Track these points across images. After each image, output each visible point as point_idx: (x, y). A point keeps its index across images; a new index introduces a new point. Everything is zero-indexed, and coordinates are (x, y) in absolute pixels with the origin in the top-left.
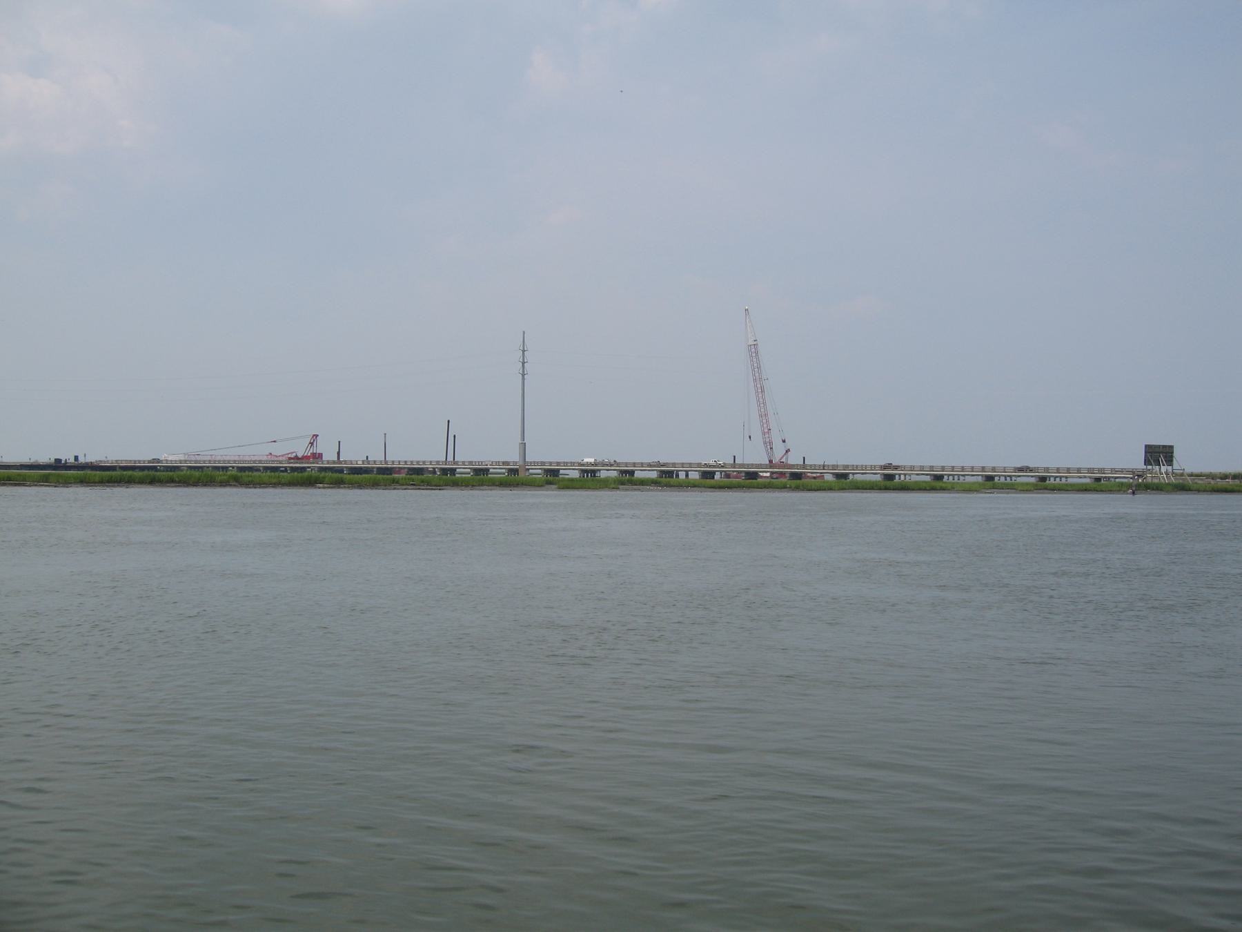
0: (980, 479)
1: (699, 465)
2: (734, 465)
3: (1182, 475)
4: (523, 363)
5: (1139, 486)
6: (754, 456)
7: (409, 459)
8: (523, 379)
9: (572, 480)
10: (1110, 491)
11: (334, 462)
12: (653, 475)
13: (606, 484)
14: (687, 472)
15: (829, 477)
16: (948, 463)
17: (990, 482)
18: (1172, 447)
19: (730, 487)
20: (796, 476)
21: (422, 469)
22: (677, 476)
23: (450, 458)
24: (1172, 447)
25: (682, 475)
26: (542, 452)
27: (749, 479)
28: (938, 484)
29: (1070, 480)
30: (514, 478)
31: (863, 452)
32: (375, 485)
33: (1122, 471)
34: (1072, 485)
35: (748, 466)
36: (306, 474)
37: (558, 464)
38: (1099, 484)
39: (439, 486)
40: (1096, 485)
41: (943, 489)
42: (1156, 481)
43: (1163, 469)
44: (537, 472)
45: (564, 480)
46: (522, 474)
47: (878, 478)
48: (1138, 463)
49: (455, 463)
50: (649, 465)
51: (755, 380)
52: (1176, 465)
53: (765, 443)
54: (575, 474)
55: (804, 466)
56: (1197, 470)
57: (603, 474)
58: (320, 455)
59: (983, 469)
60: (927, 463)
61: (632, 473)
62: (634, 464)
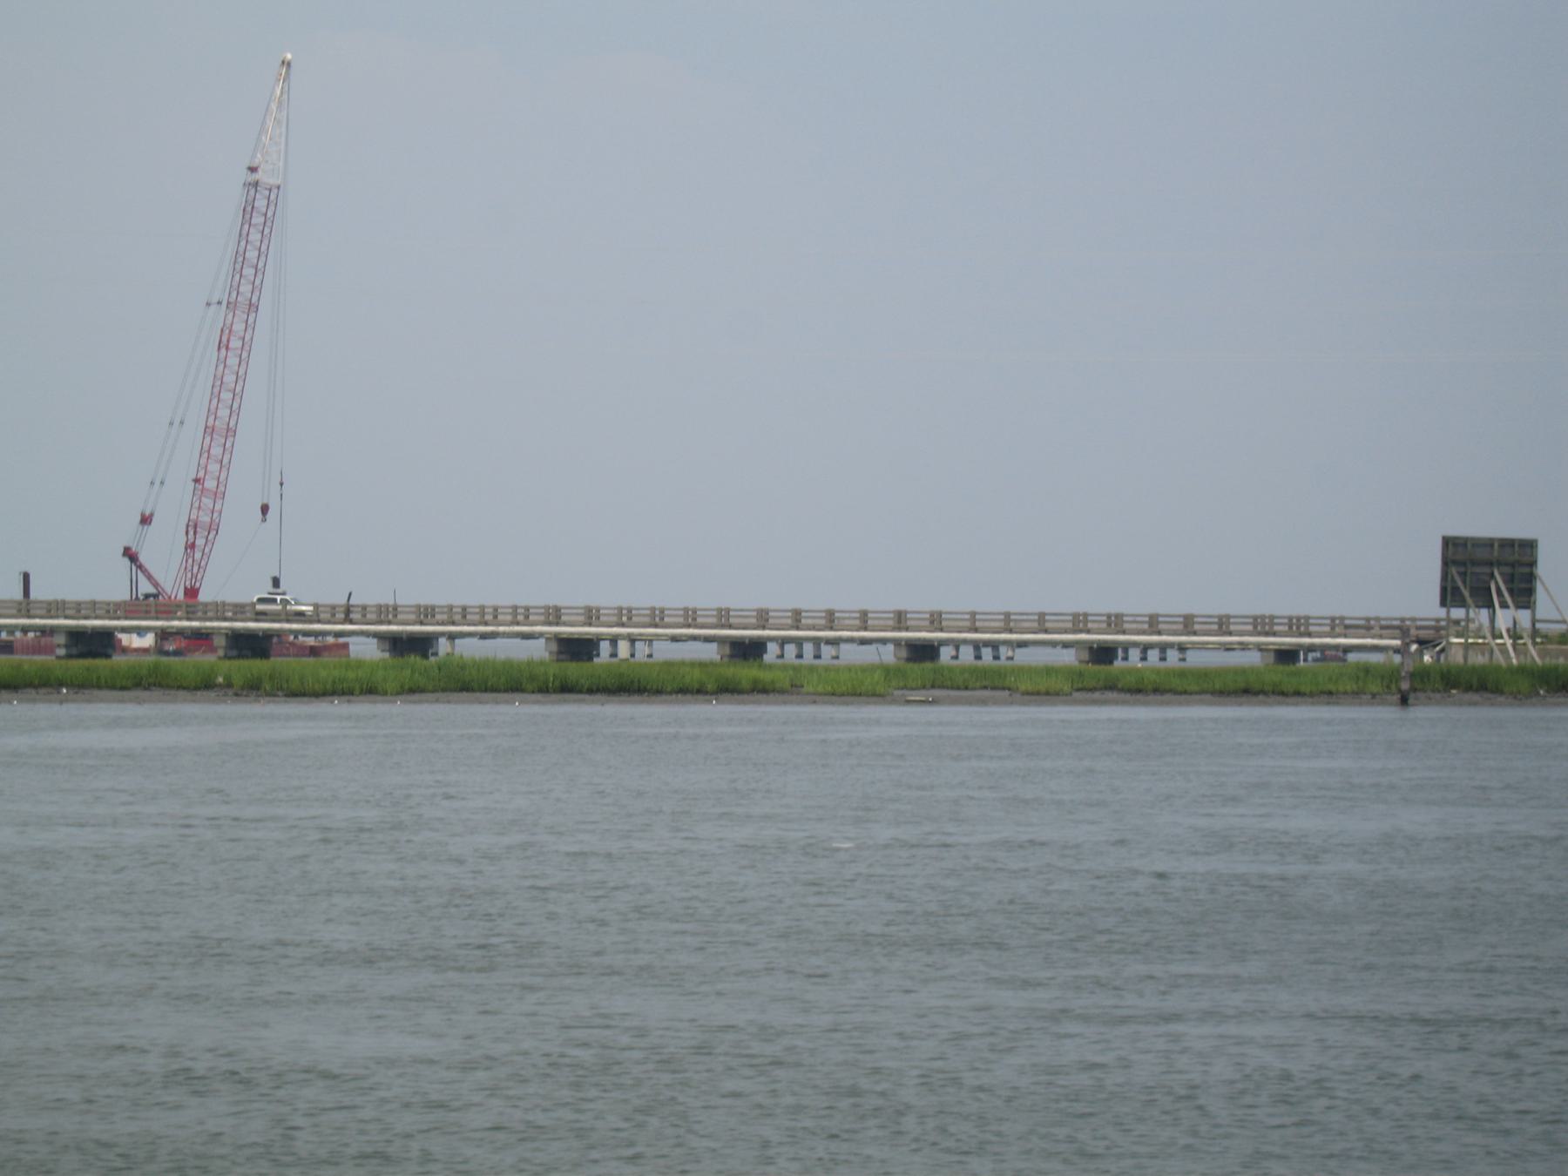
0: (888, 655)
5: (1422, 677)
10: (1327, 695)
16: (780, 600)
18: (1529, 546)
24: (1529, 546)
29: (1195, 659)
33: (1366, 627)
34: (1203, 675)
38: (1292, 671)
40: (1279, 674)
41: (761, 690)
42: (1478, 659)
43: (1504, 619)
48: (1420, 597)
52: (1544, 605)
59: (900, 620)
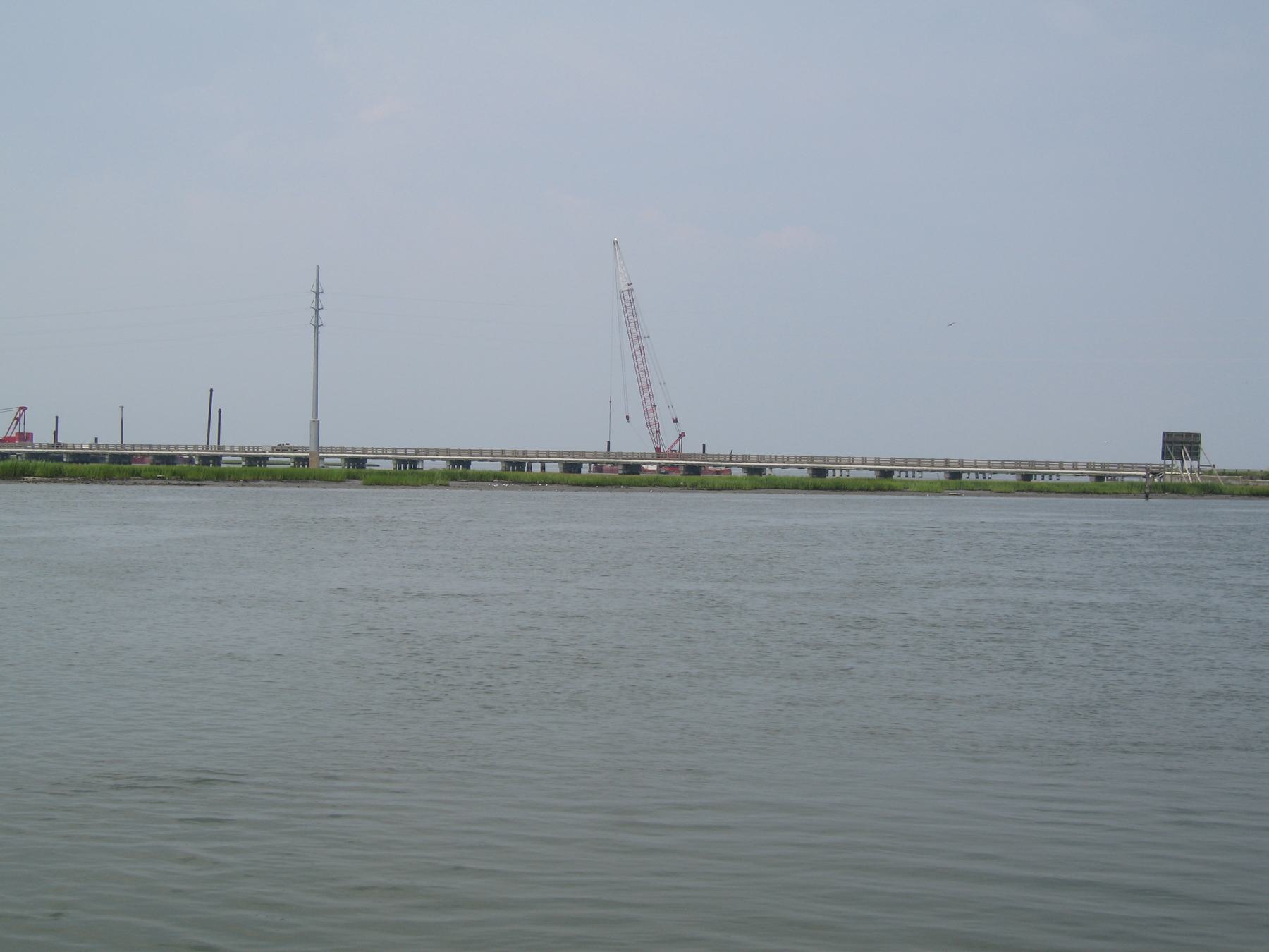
0: (942, 476)
1: (560, 454)
2: (608, 454)
3: (1211, 473)
4: (317, 310)
5: (1153, 487)
6: (633, 441)
7: (155, 442)
8: (317, 333)
9: (384, 473)
10: (1116, 494)
11: (50, 446)
12: (497, 467)
13: (430, 479)
14: (543, 463)
15: (738, 472)
16: (900, 454)
17: (956, 480)
18: (1198, 435)
19: (602, 484)
20: (694, 470)
21: (173, 457)
22: (530, 468)
23: (213, 442)
24: (1198, 435)
25: (536, 468)
26: (344, 434)
27: (629, 474)
28: (886, 482)
29: (1063, 479)
30: (302, 470)
31: (789, 439)
32: (106, 478)
33: (1132, 467)
34: (1067, 485)
35: (627, 455)
36: (9, 463)
37: (365, 450)
38: (1102, 484)
39: (198, 480)
41: (891, 489)
42: (1177, 481)
43: (1187, 465)
44: (335, 461)
45: (372, 472)
46: (314, 465)
47: (805, 473)
48: (1153, 456)
49: (220, 448)
50: (492, 453)
51: (631, 339)
52: (1203, 460)
53: (649, 425)
54: (388, 465)
55: (704, 456)
56: (1230, 467)
57: (427, 466)
58: (30, 436)
59: (947, 463)
60: (871, 453)
61: (467, 464)
62: (470, 452)
